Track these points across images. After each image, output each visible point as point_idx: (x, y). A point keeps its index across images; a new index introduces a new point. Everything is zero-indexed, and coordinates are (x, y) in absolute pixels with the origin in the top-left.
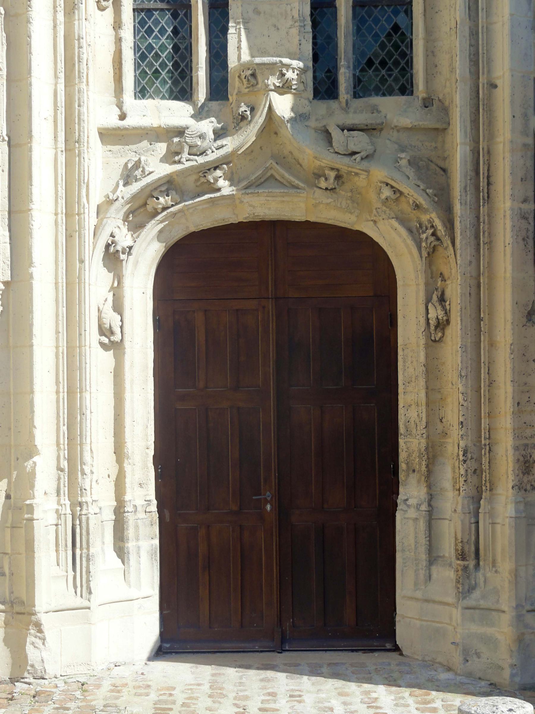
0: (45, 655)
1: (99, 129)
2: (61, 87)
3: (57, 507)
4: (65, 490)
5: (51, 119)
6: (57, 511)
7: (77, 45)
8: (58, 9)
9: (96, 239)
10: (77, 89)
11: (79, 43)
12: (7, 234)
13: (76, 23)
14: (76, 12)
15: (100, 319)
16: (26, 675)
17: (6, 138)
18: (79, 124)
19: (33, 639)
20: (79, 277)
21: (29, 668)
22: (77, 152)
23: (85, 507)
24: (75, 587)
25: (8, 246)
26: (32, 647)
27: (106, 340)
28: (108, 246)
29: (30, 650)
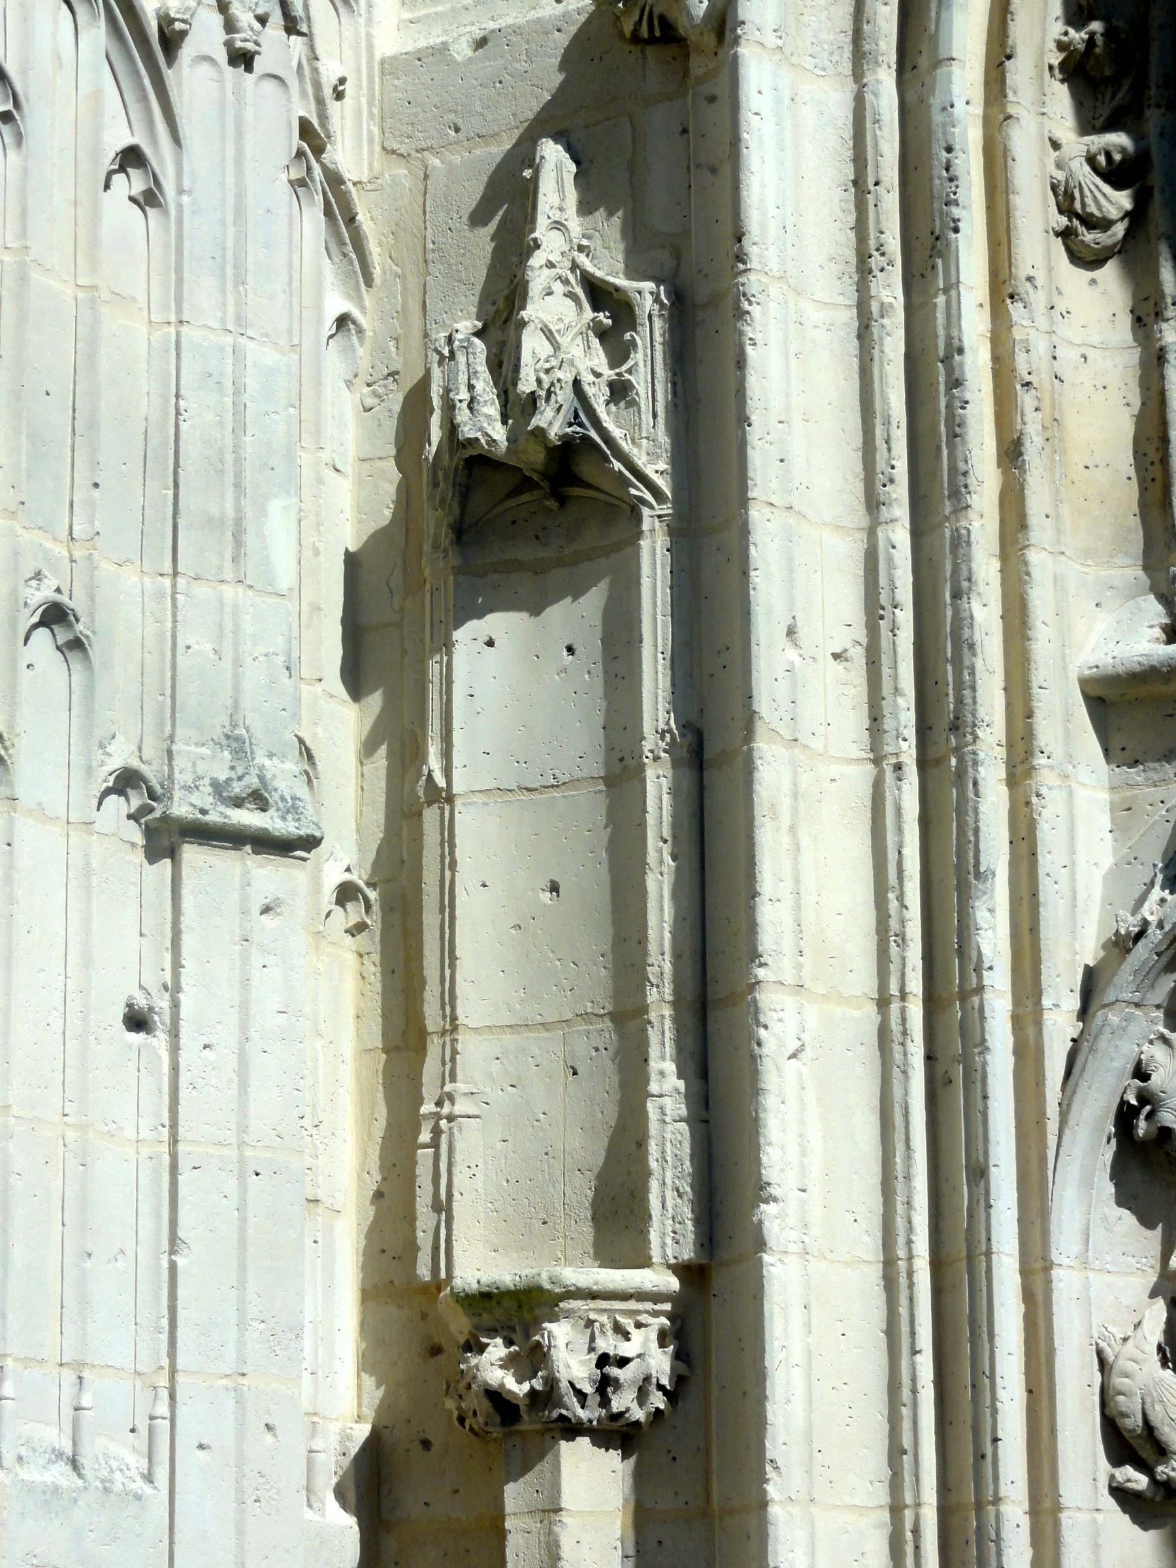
1: (1084, 683)
5: (858, 655)
8: (876, 261)
9: (1069, 1090)
10: (948, 533)
11: (950, 370)
13: (941, 300)
14: (940, 262)
15: (1105, 1396)
18: (957, 660)
22: (953, 761)
27: (1139, 1481)
28: (1125, 1116)
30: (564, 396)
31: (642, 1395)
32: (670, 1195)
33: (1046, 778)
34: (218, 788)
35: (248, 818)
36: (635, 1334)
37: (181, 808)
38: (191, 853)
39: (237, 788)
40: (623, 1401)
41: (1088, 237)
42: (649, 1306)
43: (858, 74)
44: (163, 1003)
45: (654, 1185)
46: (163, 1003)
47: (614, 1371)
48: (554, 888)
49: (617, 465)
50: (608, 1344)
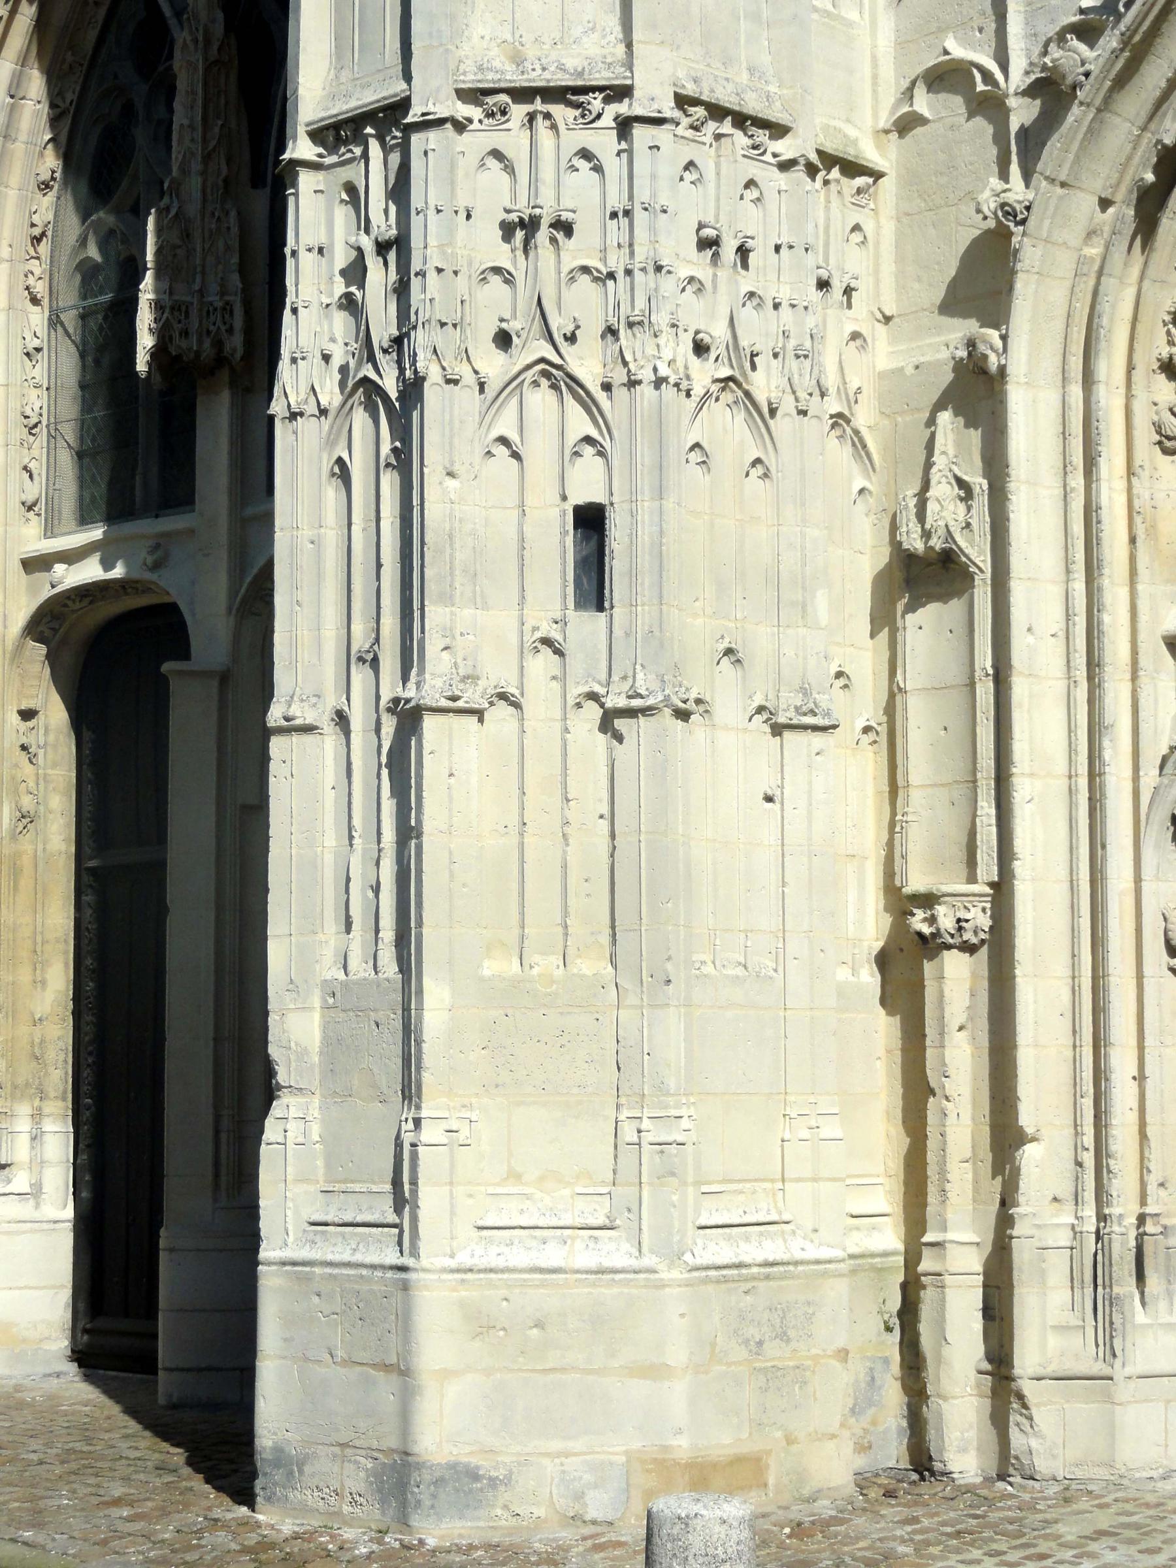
0: (1034, 1443)
2: (1079, 586)
3: (1072, 1220)
4: (1089, 1195)
5: (1062, 634)
6: (1073, 1227)
7: (1094, 520)
12: (993, 811)
16: (1011, 1471)
17: (991, 671)
19: (1019, 1418)
20: (1101, 872)
21: (1013, 1461)
23: (1108, 1224)
24: (1097, 1345)
25: (994, 829)
26: (1016, 1429)
29: (1014, 1433)
30: (942, 532)
31: (975, 933)
32: (985, 855)
33: (1144, 679)
34: (797, 709)
35: (809, 720)
36: (972, 909)
37: (782, 719)
38: (787, 735)
39: (804, 709)
40: (968, 936)
41: (1168, 444)
42: (977, 898)
43: (1064, 387)
44: (778, 793)
45: (979, 851)
46: (778, 793)
47: (963, 924)
48: (945, 729)
49: (964, 559)
50: (962, 914)
